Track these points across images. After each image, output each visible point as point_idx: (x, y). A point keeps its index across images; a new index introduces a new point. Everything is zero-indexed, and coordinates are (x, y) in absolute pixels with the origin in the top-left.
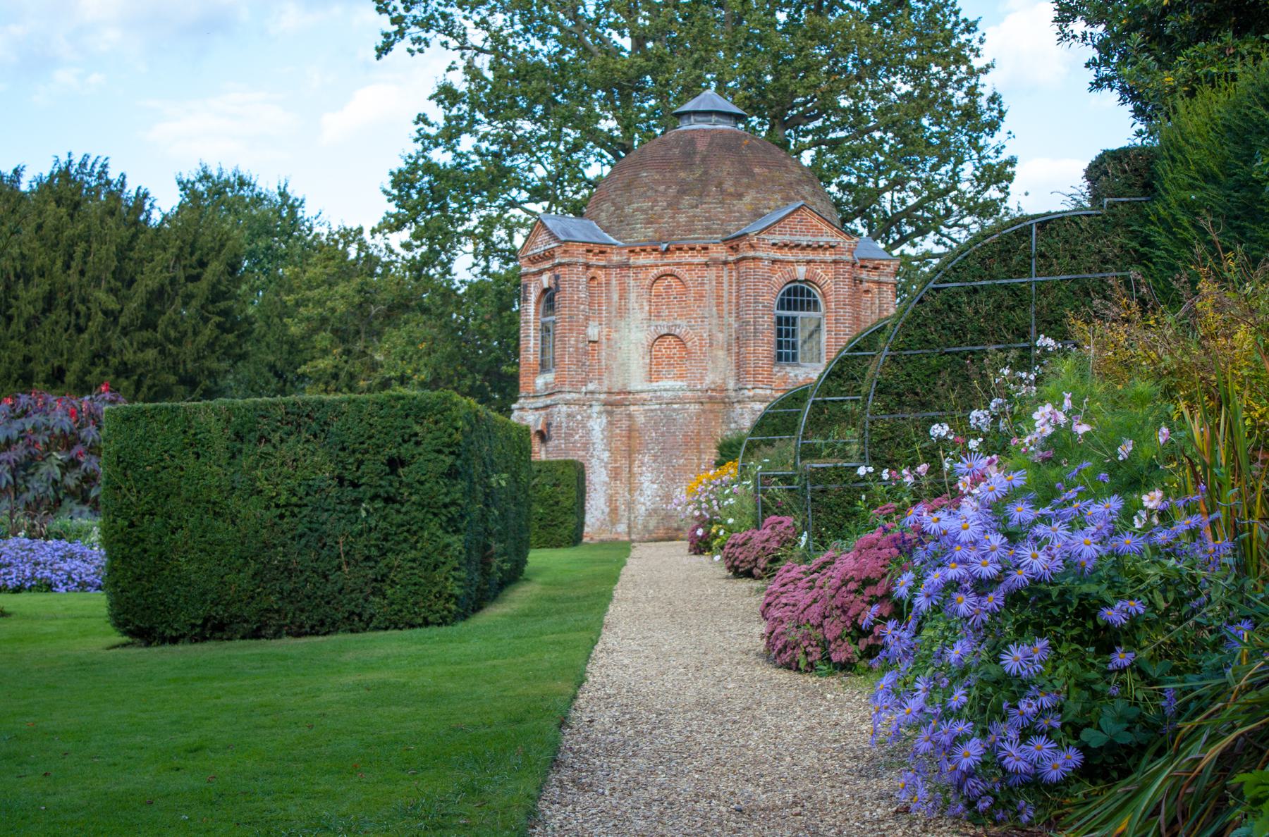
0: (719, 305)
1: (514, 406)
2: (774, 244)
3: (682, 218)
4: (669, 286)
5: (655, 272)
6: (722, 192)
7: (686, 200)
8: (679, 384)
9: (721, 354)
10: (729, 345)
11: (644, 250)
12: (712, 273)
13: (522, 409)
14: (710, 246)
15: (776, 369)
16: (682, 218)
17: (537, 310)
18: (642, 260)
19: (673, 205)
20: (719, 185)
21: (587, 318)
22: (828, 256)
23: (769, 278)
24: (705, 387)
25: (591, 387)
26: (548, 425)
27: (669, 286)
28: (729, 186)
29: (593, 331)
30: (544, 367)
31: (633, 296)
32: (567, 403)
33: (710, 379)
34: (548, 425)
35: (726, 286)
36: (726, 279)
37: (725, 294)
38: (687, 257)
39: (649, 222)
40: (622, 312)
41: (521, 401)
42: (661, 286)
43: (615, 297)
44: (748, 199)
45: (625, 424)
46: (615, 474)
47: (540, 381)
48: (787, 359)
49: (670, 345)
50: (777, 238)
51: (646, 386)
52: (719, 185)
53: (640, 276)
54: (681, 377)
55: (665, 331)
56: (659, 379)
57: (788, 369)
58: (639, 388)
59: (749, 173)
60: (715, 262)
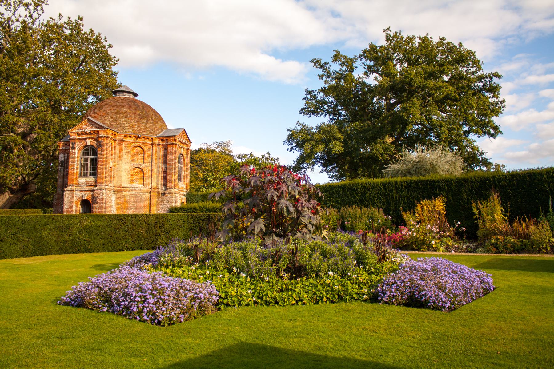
1: (65, 189)
4: (138, 150)
6: (153, 120)
7: (143, 121)
18: (128, 140)
20: (151, 118)
27: (138, 150)
31: (124, 152)
38: (145, 141)
39: (130, 126)
40: (120, 158)
44: (159, 124)
51: (128, 186)
52: (151, 118)
56: (132, 183)
58: (126, 186)
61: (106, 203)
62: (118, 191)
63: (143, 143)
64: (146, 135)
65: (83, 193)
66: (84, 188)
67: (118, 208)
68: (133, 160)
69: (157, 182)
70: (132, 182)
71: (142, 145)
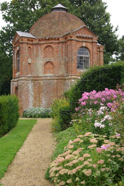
0: (62, 54)
1: (11, 81)
2: (77, 37)
3: (53, 31)
5: (45, 45)
7: (54, 27)
8: (52, 75)
9: (63, 66)
10: (65, 64)
11: (43, 40)
12: (61, 45)
13: (13, 81)
14: (60, 38)
15: (77, 70)
16: (53, 31)
18: (42, 42)
19: (50, 28)
21: (28, 57)
22: (91, 41)
23: (76, 46)
24: (58, 76)
25: (29, 75)
26: (18, 85)
28: (64, 23)
29: (30, 61)
30: (18, 70)
31: (40, 52)
32: (22, 80)
33: (61, 73)
34: (18, 85)
35: (64, 48)
36: (64, 46)
37: (64, 51)
38: (54, 41)
40: (37, 56)
41: (13, 79)
42: (47, 49)
43: (35, 52)
45: (38, 85)
46: (35, 98)
47: (17, 74)
48: (80, 68)
49: (49, 65)
50: (78, 35)
51: (43, 75)
53: (42, 46)
54: (53, 73)
55: (48, 61)
57: (81, 70)
58: (41, 76)
59: (70, 21)
60: (61, 43)
63: (52, 43)
69: (62, 72)
71: (52, 45)
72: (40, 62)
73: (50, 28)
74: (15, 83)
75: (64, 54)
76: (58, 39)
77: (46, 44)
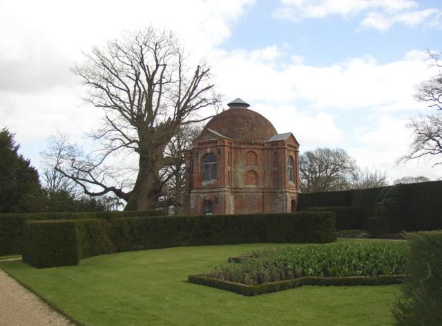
5: (247, 150)
8: (255, 186)
17: (201, 162)
19: (251, 130)
31: (239, 158)
32: (225, 191)
38: (257, 147)
40: (236, 162)
47: (204, 184)
58: (242, 187)
61: (225, 203)
62: (235, 192)
64: (258, 141)
65: (206, 194)
66: (206, 191)
67: (236, 207)
68: (248, 164)
70: (247, 183)
71: (256, 151)
72: (241, 170)
73: (251, 130)
74: (202, 195)
75: (270, 163)
76: (263, 144)
77: (247, 148)
